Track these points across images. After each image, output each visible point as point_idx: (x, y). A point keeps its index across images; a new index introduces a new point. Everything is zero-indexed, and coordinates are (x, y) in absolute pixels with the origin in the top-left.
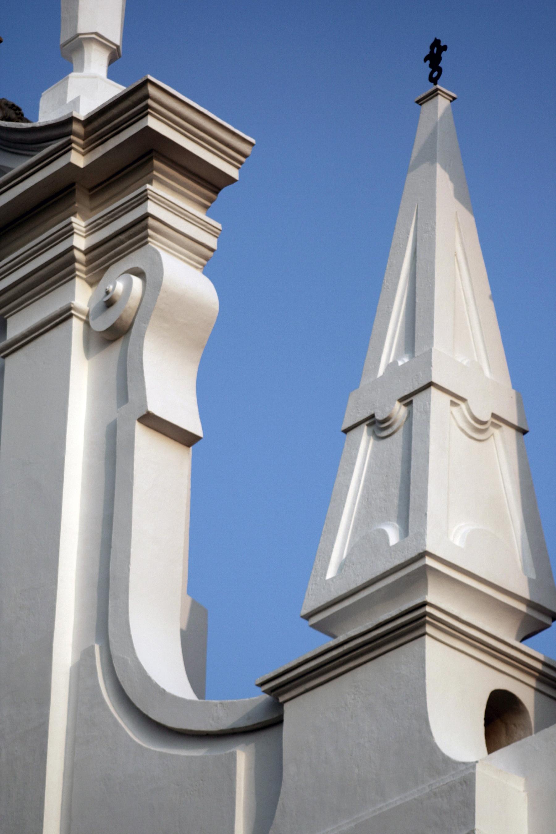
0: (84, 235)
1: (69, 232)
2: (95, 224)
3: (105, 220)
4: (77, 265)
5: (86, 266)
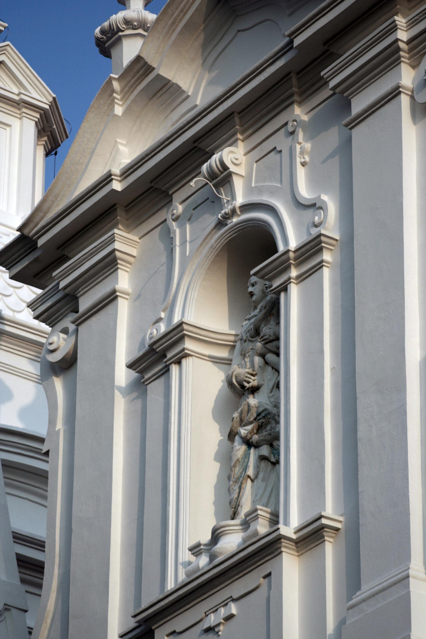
0: (405, 29)
1: (394, 28)
2: (413, 20)
3: (421, 16)
4: (402, 53)
5: (408, 53)
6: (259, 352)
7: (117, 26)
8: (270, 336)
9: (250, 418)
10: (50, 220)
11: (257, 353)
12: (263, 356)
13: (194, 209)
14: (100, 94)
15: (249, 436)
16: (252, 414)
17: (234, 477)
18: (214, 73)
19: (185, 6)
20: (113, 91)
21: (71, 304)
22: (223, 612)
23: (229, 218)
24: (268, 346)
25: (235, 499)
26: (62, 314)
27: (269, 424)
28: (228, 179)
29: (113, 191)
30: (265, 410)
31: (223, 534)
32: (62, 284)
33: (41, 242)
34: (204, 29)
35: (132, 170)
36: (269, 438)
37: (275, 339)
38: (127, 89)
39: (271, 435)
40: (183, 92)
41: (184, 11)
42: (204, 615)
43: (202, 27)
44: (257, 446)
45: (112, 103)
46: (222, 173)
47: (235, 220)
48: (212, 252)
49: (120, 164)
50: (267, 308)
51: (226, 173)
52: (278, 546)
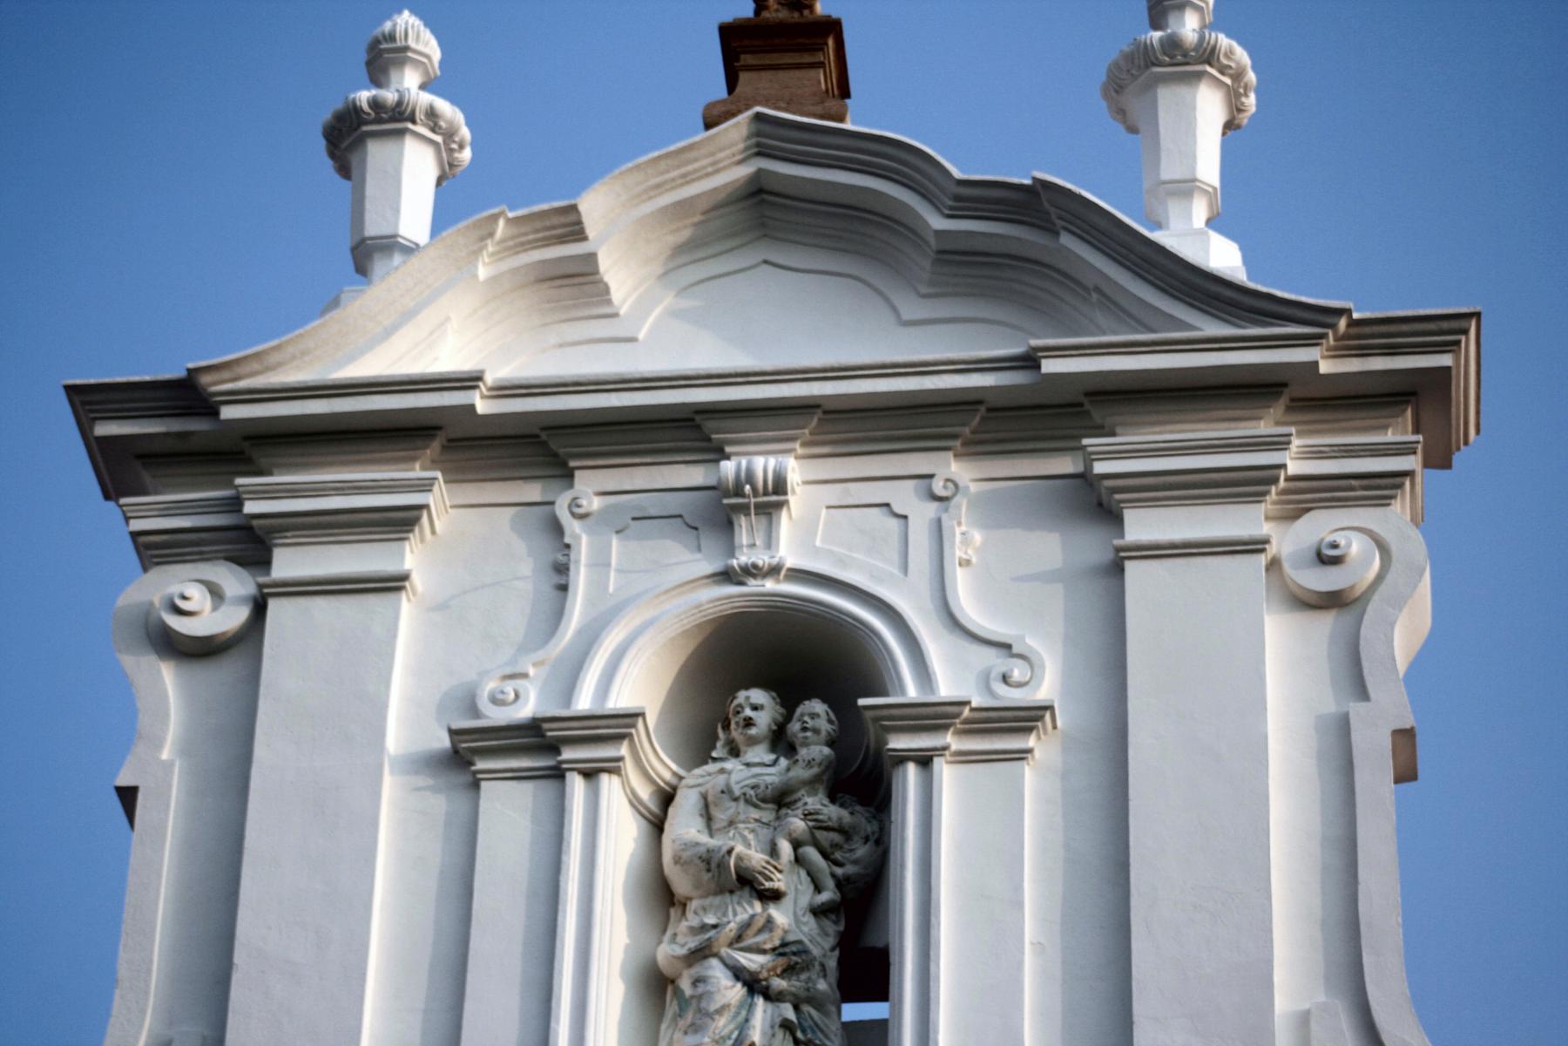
3: (1334, 451)
6: (794, 835)
7: (413, 112)
8: (830, 819)
9: (765, 943)
10: (278, 387)
11: (790, 835)
12: (796, 845)
13: (634, 519)
14: (467, 227)
15: (764, 974)
16: (771, 939)
17: (714, 1033)
18: (686, 303)
19: (695, 171)
20: (491, 235)
21: (243, 546)
23: (754, 576)
24: (820, 835)
26: (201, 553)
28: (770, 510)
29: (471, 408)
30: (799, 942)
32: (250, 507)
33: (228, 413)
34: (695, 225)
35: (524, 391)
36: (803, 994)
38: (511, 243)
40: (609, 302)
41: (688, 179)
43: (698, 218)
44: (769, 996)
45: (477, 252)
46: (766, 493)
47: (770, 585)
48: (693, 615)
49: (436, 359)
50: (823, 767)
51: (774, 498)
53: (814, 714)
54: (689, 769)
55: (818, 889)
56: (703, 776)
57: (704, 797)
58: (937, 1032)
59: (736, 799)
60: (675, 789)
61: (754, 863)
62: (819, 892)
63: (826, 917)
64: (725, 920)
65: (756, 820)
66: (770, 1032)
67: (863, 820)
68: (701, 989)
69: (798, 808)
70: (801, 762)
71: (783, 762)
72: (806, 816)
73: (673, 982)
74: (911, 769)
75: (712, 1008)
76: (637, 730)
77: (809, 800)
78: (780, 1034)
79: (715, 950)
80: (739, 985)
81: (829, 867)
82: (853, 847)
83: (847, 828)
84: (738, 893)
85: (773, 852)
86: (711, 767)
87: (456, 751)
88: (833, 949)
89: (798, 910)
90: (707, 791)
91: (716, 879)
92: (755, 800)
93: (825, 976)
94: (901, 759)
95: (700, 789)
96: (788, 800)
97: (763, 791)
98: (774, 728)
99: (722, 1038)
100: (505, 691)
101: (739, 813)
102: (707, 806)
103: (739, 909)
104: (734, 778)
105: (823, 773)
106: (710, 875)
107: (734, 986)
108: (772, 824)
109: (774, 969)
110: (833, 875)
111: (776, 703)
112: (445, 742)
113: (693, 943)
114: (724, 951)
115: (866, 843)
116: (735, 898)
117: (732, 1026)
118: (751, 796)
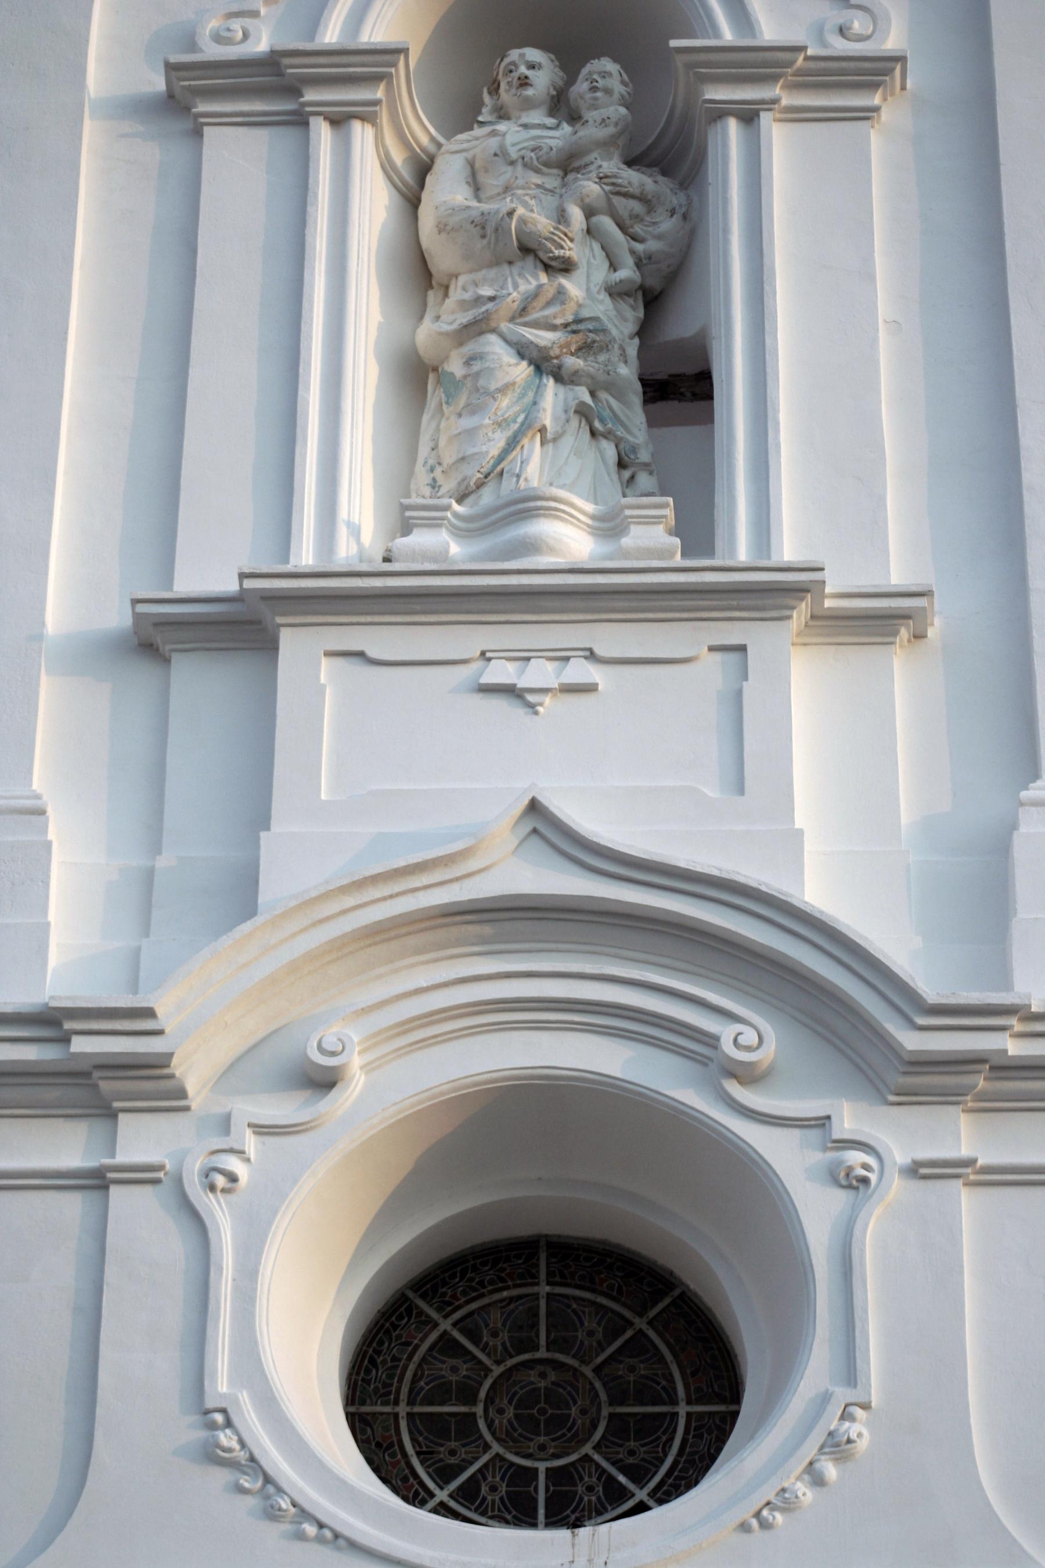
6: (587, 200)
8: (630, 183)
9: (555, 317)
11: (582, 200)
12: (589, 213)
15: (556, 351)
16: (563, 312)
22: (579, 671)
24: (617, 200)
25: (492, 457)
27: (605, 351)
31: (551, 514)
36: (602, 377)
37: (639, 195)
39: (609, 374)
42: (479, 653)
50: (619, 127)
52: (791, 602)
53: (605, 72)
54: (448, 137)
55: (613, 267)
56: (469, 141)
57: (471, 164)
58: (776, 411)
59: (512, 163)
60: (432, 159)
61: (540, 227)
62: (615, 270)
63: (623, 300)
64: (505, 292)
65: (538, 186)
66: (564, 417)
67: (668, 191)
68: (476, 367)
69: (591, 172)
70: (591, 122)
71: (566, 128)
72: (601, 179)
73: (435, 369)
74: (733, 125)
75: (493, 387)
76: (397, 71)
77: (605, 164)
78: (575, 421)
79: (493, 324)
80: (524, 364)
81: (628, 241)
82: (657, 220)
83: (649, 197)
84: (519, 264)
85: (562, 217)
86: (478, 131)
87: (171, 95)
88: (631, 338)
89: (592, 285)
90: (474, 157)
91: (492, 246)
92: (535, 163)
93: (626, 362)
94: (719, 113)
95: (465, 154)
96: (576, 164)
97: (547, 153)
98: (554, 93)
99: (505, 420)
100: (232, 28)
101: (516, 178)
102: (474, 174)
103: (520, 281)
104: (509, 140)
105: (621, 133)
106: (485, 241)
107: (517, 364)
108: (558, 191)
109: (568, 345)
110: (632, 252)
111: (555, 66)
112: (158, 83)
113: (464, 318)
114: (505, 326)
115: (672, 216)
116: (515, 270)
117: (517, 408)
118: (531, 158)
